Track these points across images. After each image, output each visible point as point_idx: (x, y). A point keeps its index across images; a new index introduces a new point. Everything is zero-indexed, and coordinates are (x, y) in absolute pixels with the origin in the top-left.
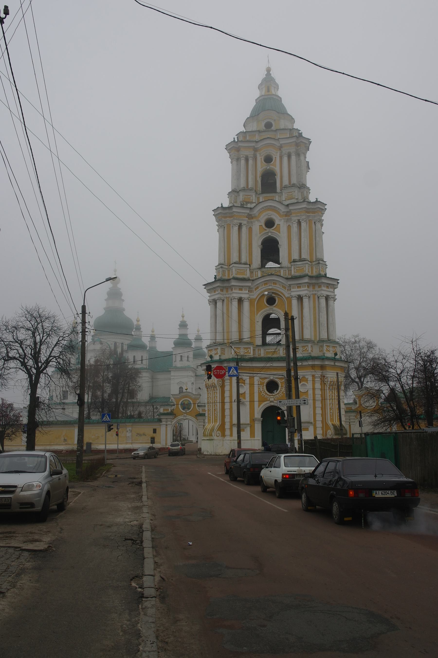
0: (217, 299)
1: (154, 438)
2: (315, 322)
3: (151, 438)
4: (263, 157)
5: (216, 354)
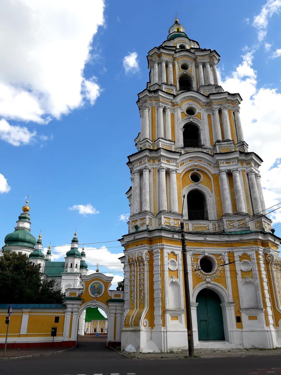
0: (144, 169)
1: (56, 328)
3: (53, 329)
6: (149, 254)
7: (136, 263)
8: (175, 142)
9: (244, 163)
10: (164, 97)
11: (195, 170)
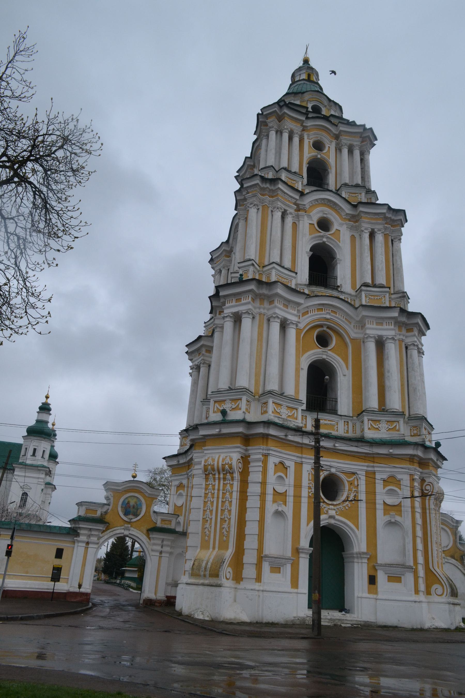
0: (245, 313)
2: (402, 385)
3: (54, 569)
4: (312, 142)
5: (233, 409)
6: (242, 462)
7: (219, 473)
8: (296, 273)
9: (403, 329)
10: (285, 193)
11: (324, 326)
